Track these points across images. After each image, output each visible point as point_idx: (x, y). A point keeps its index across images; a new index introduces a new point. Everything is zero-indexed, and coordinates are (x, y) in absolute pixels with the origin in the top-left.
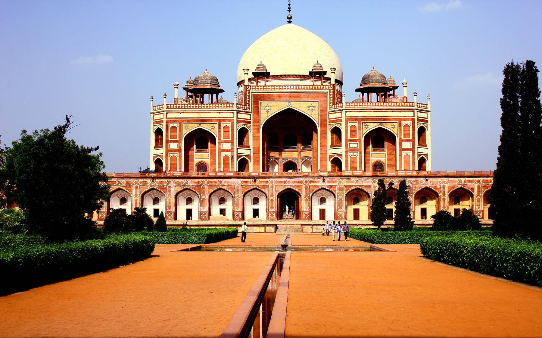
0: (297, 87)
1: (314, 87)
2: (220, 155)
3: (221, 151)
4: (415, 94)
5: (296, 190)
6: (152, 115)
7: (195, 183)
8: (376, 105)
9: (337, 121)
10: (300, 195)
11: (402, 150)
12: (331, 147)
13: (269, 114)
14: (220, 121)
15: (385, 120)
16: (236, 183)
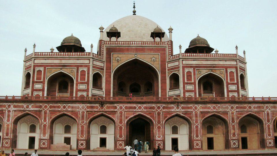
0: (142, 43)
1: (155, 43)
2: (76, 94)
3: (78, 91)
4: (237, 47)
5: (148, 116)
6: (25, 63)
7: (36, 107)
8: (206, 56)
9: (175, 68)
10: (152, 122)
11: (228, 91)
12: (170, 89)
13: (119, 63)
14: (78, 67)
15: (214, 67)
16: (81, 108)
